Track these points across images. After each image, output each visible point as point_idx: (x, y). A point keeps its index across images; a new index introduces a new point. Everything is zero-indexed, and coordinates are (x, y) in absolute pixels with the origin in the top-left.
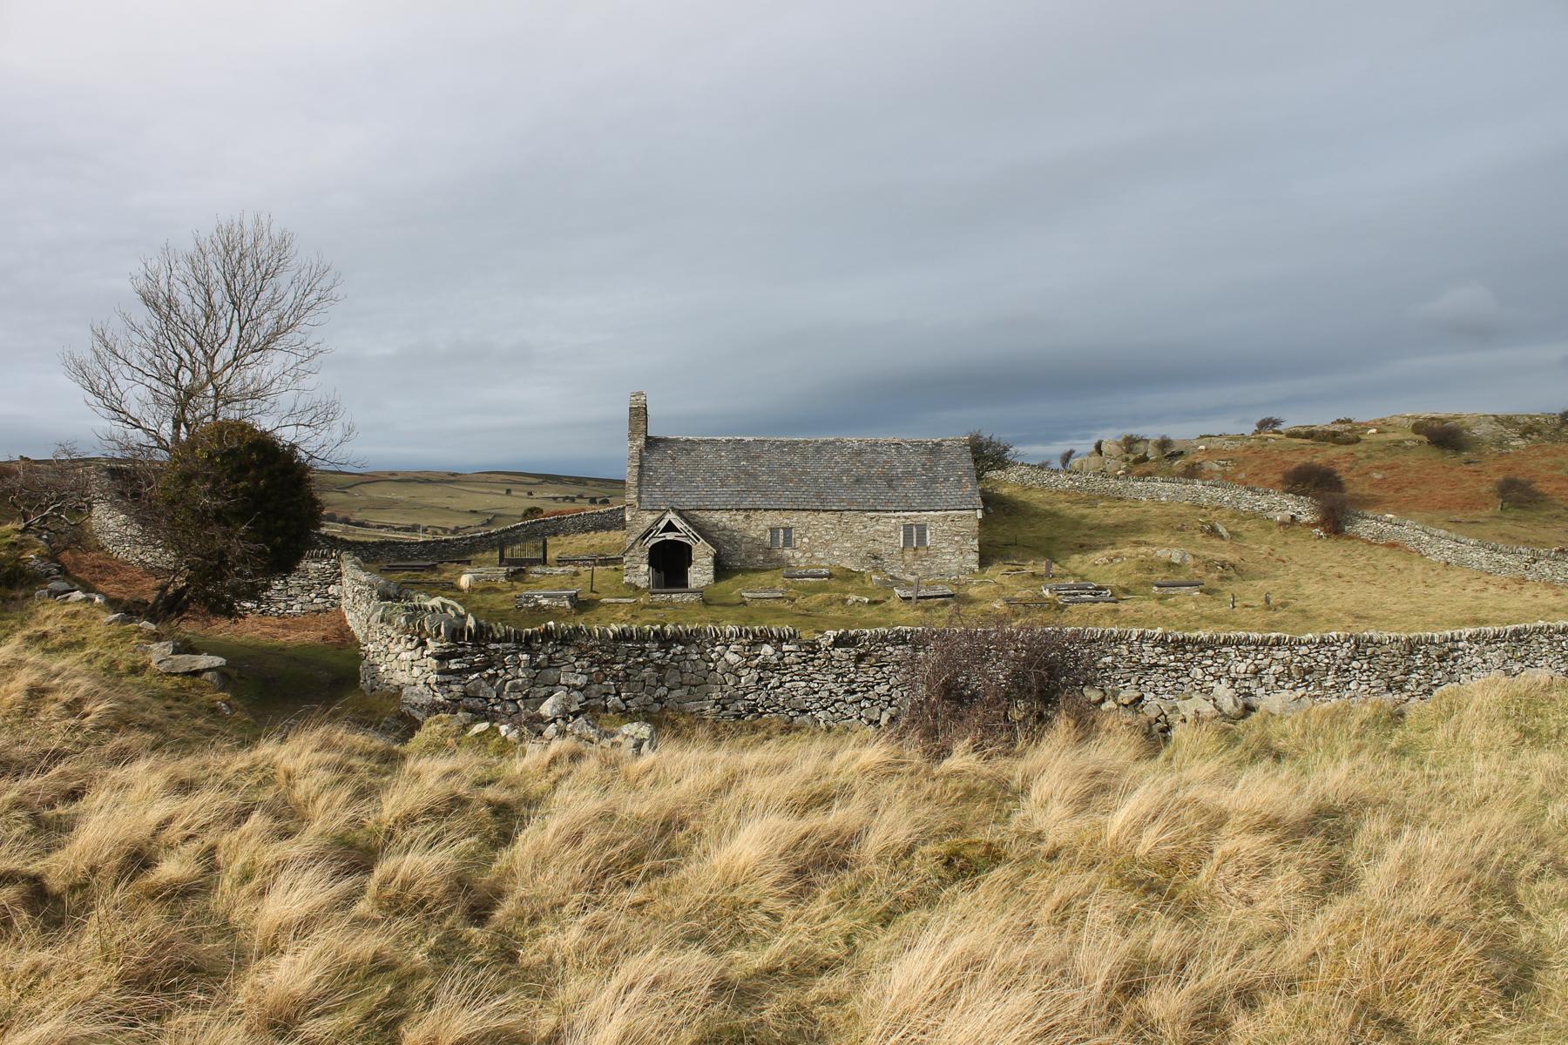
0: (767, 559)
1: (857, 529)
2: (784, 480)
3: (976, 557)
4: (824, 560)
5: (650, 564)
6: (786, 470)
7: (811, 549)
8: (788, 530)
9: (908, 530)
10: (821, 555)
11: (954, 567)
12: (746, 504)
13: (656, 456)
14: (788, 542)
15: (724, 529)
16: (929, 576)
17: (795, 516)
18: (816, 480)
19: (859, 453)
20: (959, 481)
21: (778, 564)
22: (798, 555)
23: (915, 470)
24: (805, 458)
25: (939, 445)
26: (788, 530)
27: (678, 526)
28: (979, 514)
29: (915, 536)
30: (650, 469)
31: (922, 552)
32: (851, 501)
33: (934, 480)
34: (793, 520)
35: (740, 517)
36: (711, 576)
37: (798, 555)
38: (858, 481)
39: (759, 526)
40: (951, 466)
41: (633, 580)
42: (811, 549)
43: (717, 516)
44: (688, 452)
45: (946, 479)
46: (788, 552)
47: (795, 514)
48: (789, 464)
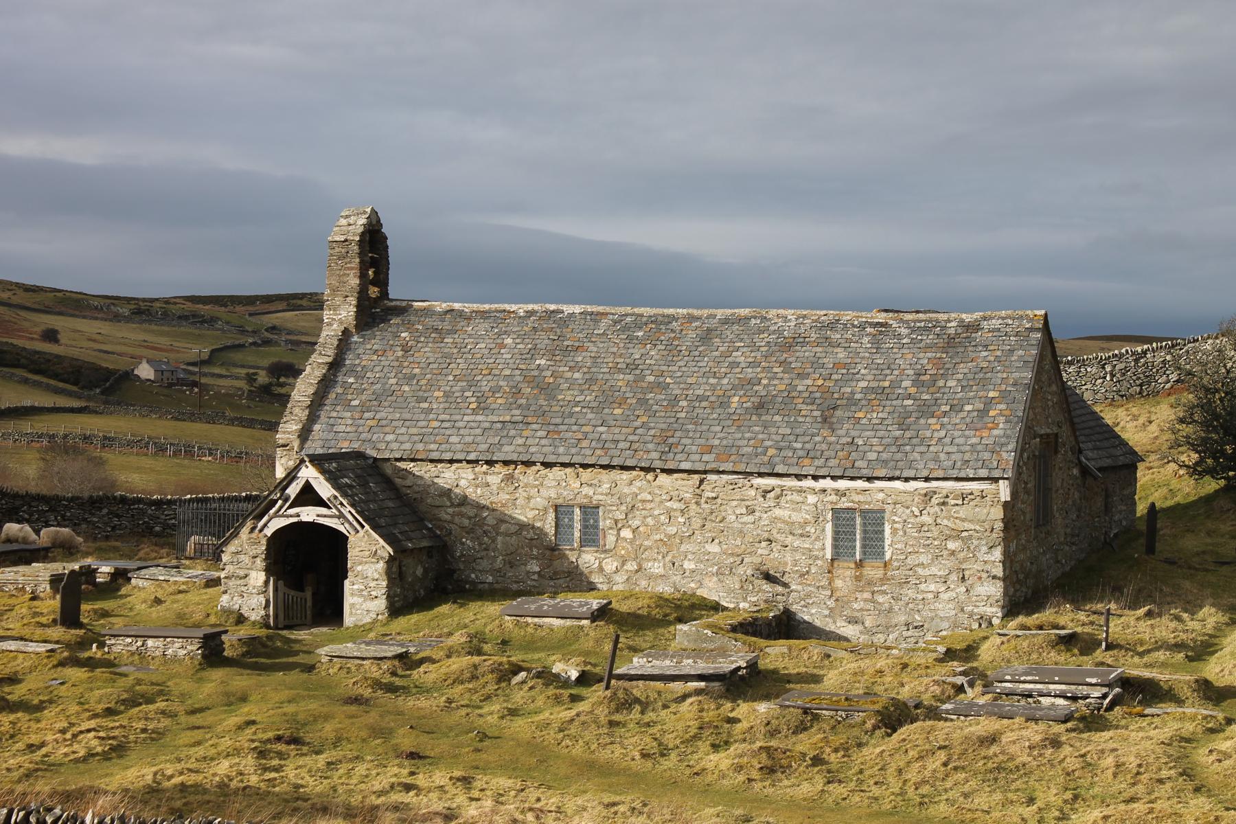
0: (538, 565)
1: (733, 513)
2: (609, 398)
3: (995, 590)
4: (660, 579)
5: (268, 571)
6: (621, 380)
7: (638, 553)
8: (590, 511)
10: (656, 568)
12: (508, 452)
13: (376, 344)
14: (591, 537)
15: (464, 501)
16: (888, 628)
18: (676, 399)
20: (983, 413)
21: (578, 581)
22: (610, 565)
23: (895, 384)
24: (672, 351)
25: (974, 327)
26: (590, 511)
28: (1004, 491)
29: (858, 534)
30: (352, 371)
31: (873, 571)
32: (726, 452)
33: (926, 410)
35: (495, 477)
36: (381, 604)
37: (610, 565)
38: (761, 407)
39: (530, 500)
40: (981, 378)
41: (236, 603)
42: (638, 553)
45: (956, 408)
47: (605, 476)
48: (632, 367)
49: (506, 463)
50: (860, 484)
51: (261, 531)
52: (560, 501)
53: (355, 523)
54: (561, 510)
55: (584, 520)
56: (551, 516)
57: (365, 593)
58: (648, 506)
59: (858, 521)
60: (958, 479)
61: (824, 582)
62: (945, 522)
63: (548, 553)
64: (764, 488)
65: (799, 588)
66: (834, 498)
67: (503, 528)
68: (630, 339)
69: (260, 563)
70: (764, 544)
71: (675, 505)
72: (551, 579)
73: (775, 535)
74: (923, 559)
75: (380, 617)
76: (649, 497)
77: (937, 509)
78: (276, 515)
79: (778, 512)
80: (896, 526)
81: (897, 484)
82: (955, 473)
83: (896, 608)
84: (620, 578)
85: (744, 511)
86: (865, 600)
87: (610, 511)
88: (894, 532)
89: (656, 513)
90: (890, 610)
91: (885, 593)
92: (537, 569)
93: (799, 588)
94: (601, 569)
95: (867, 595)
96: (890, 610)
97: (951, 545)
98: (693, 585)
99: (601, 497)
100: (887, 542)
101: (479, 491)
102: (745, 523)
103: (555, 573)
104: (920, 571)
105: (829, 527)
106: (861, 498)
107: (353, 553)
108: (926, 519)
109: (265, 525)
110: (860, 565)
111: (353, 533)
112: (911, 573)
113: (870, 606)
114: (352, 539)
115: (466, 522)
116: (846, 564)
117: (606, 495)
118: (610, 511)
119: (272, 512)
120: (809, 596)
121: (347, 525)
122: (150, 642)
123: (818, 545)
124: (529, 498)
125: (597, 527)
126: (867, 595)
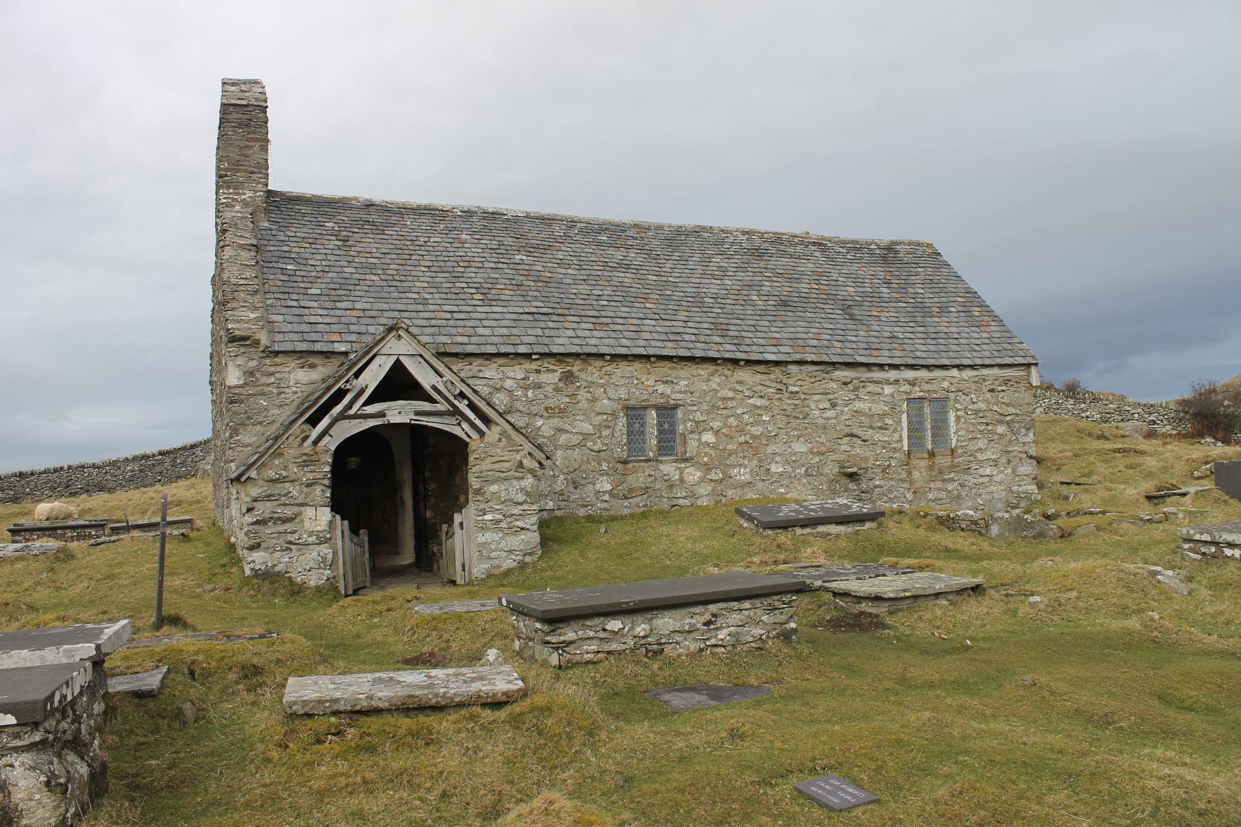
1: (817, 408)
5: (337, 506)
7: (722, 460)
9: (915, 403)
10: (742, 475)
11: (999, 492)
14: (668, 444)
17: (685, 377)
19: (758, 253)
26: (667, 410)
27: (425, 378)
31: (943, 461)
34: (683, 384)
35: (551, 377)
37: (693, 475)
41: (281, 561)
42: (722, 460)
43: (491, 371)
44: (379, 229)
45: (943, 310)
46: (668, 468)
49: (560, 357)
50: (923, 373)
51: (316, 443)
52: (632, 403)
53: (478, 422)
54: (634, 412)
55: (660, 424)
56: (622, 421)
57: (503, 525)
58: (730, 404)
60: (1001, 366)
61: (904, 475)
62: (995, 408)
63: (620, 466)
64: (844, 380)
65: (882, 482)
66: (907, 388)
67: (563, 438)
68: (600, 243)
69: (322, 493)
70: (846, 440)
71: (759, 402)
72: (626, 498)
73: (856, 431)
74: (981, 444)
75: (528, 559)
76: (730, 394)
77: (989, 395)
78: (342, 416)
79: (858, 405)
80: (959, 413)
81: (955, 372)
82: (999, 361)
83: (963, 494)
84: (704, 490)
85: (827, 405)
86: (939, 489)
87: (691, 412)
88: (958, 418)
89: (739, 411)
90: (959, 497)
91: (952, 480)
92: (609, 487)
93: (882, 482)
94: (682, 480)
95: (939, 484)
96: (959, 497)
97: (1000, 429)
98: (782, 490)
99: (679, 396)
100: (953, 430)
101: (530, 394)
102: (828, 419)
103: (631, 490)
104: (978, 455)
106: (926, 387)
108: (982, 406)
110: (932, 454)
111: (475, 435)
112: (972, 459)
113: (943, 495)
114: (475, 444)
116: (920, 455)
117: (685, 392)
118: (691, 412)
119: (338, 408)
120: (890, 490)
121: (465, 425)
122: (666, 622)
123: (896, 436)
124: (594, 400)
125: (673, 432)
126: (939, 484)
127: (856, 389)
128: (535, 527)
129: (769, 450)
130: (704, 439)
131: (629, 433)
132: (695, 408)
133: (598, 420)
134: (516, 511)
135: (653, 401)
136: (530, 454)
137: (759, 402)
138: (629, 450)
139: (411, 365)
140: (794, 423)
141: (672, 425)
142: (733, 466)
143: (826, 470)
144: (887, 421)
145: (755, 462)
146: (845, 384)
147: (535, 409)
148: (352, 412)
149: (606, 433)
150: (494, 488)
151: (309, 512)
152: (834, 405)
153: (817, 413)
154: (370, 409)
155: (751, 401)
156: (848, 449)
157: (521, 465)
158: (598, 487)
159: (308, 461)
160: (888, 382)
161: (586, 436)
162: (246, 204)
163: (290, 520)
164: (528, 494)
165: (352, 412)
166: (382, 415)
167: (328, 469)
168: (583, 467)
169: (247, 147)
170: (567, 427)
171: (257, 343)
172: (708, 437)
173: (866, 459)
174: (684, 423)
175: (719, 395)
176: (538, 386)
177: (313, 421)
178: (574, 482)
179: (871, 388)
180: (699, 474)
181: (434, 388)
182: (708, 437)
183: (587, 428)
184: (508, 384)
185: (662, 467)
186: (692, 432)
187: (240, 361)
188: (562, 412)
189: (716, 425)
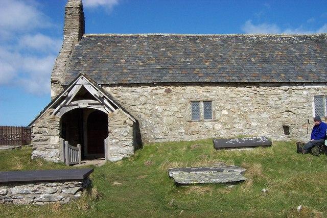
5: (63, 135)
14: (208, 114)
26: (208, 103)
27: (92, 91)
34: (215, 92)
36: (132, 148)
37: (218, 126)
46: (208, 124)
51: (55, 114)
54: (195, 103)
55: (205, 107)
56: (190, 106)
57: (119, 144)
58: (234, 99)
59: (325, 100)
63: (188, 123)
66: (314, 91)
67: (166, 113)
69: (56, 132)
70: (285, 113)
71: (246, 98)
73: (290, 109)
76: (234, 96)
78: (64, 105)
79: (291, 99)
92: (184, 131)
103: (192, 132)
105: (313, 103)
107: (111, 123)
109: (58, 111)
111: (110, 112)
115: (148, 112)
121: (106, 108)
122: (15, 190)
123: (309, 111)
124: (179, 99)
127: (291, 93)
128: (131, 145)
129: (251, 117)
130: (223, 113)
131: (193, 111)
132: (219, 101)
133: (180, 106)
134: (124, 139)
135: (202, 99)
136: (129, 118)
137: (246, 98)
138: (193, 117)
139: (87, 87)
140: (262, 106)
141: (210, 107)
142: (235, 123)
143: (277, 125)
144: (305, 105)
145: (245, 121)
146: (286, 91)
147: (155, 103)
148: (67, 104)
149: (183, 111)
150: (116, 130)
151: (52, 138)
152: (280, 99)
153: (272, 102)
154: (73, 103)
155: (243, 98)
156: (286, 116)
157: (125, 122)
158: (179, 131)
159: (52, 121)
160: (305, 90)
161: (175, 112)
162: (72, 39)
163: (46, 140)
164: (128, 133)
165: (67, 104)
166: (77, 105)
167: (58, 123)
168: (174, 123)
169: (72, 20)
170: (167, 109)
171: (59, 83)
172: (225, 112)
173: (295, 121)
174: (215, 107)
175: (230, 96)
176: (156, 94)
177: (55, 107)
178: (170, 129)
179: (297, 92)
180: (221, 126)
181: (95, 95)
182: (225, 112)
183: (176, 109)
184: (146, 94)
185: (205, 123)
186: (218, 110)
187: (54, 88)
188: (166, 104)
189: (228, 107)
